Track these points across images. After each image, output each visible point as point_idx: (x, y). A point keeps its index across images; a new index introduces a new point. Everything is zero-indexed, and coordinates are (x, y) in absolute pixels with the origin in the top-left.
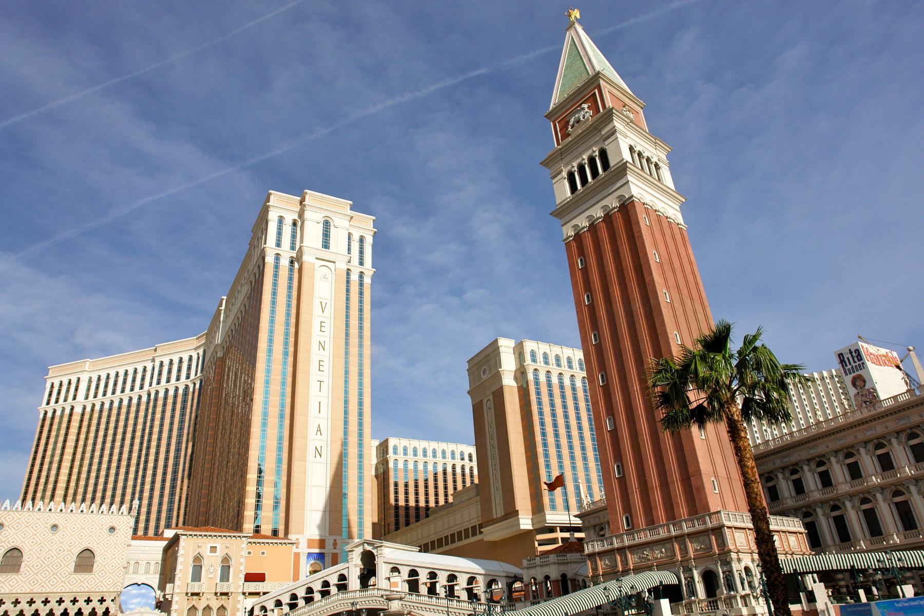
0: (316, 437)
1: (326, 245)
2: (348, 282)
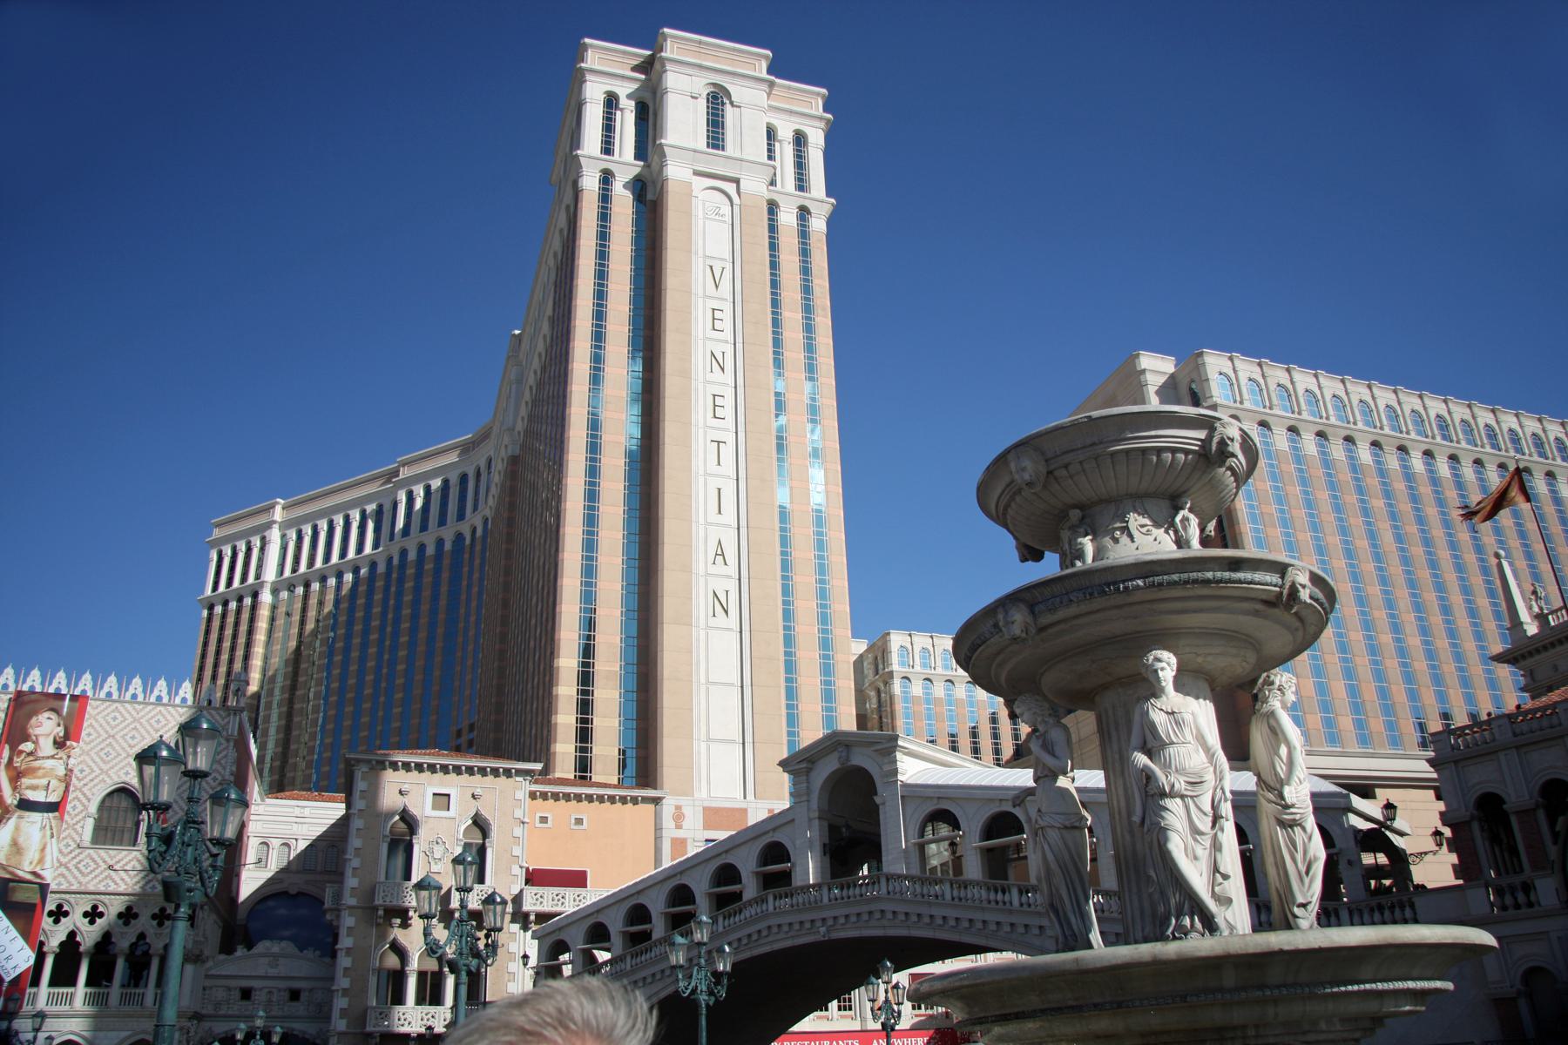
0: (712, 569)
2: (773, 228)
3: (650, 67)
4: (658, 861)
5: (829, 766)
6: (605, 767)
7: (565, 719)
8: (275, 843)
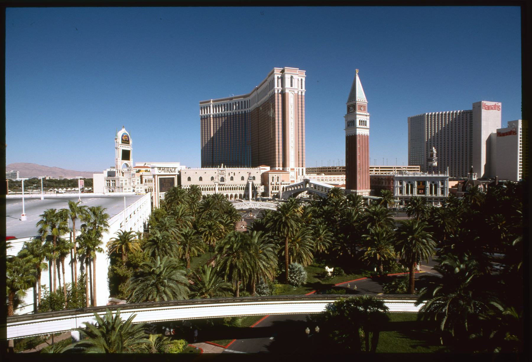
1: (292, 86)
3: (283, 71)
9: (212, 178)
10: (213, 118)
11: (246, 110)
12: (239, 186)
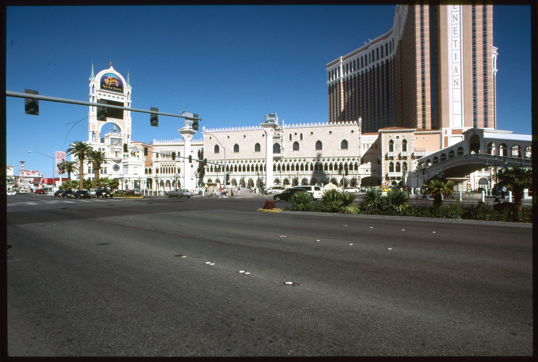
4: (441, 147)
5: (472, 134)
6: (429, 125)
7: (420, 119)
8: (366, 145)
9: (258, 147)
10: (344, 83)
11: (388, 57)
12: (311, 161)
